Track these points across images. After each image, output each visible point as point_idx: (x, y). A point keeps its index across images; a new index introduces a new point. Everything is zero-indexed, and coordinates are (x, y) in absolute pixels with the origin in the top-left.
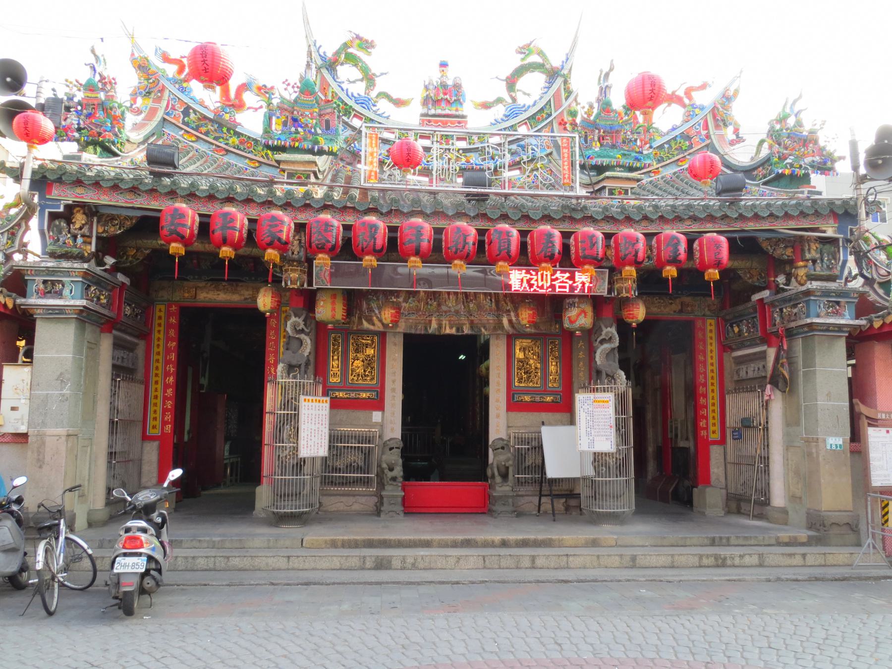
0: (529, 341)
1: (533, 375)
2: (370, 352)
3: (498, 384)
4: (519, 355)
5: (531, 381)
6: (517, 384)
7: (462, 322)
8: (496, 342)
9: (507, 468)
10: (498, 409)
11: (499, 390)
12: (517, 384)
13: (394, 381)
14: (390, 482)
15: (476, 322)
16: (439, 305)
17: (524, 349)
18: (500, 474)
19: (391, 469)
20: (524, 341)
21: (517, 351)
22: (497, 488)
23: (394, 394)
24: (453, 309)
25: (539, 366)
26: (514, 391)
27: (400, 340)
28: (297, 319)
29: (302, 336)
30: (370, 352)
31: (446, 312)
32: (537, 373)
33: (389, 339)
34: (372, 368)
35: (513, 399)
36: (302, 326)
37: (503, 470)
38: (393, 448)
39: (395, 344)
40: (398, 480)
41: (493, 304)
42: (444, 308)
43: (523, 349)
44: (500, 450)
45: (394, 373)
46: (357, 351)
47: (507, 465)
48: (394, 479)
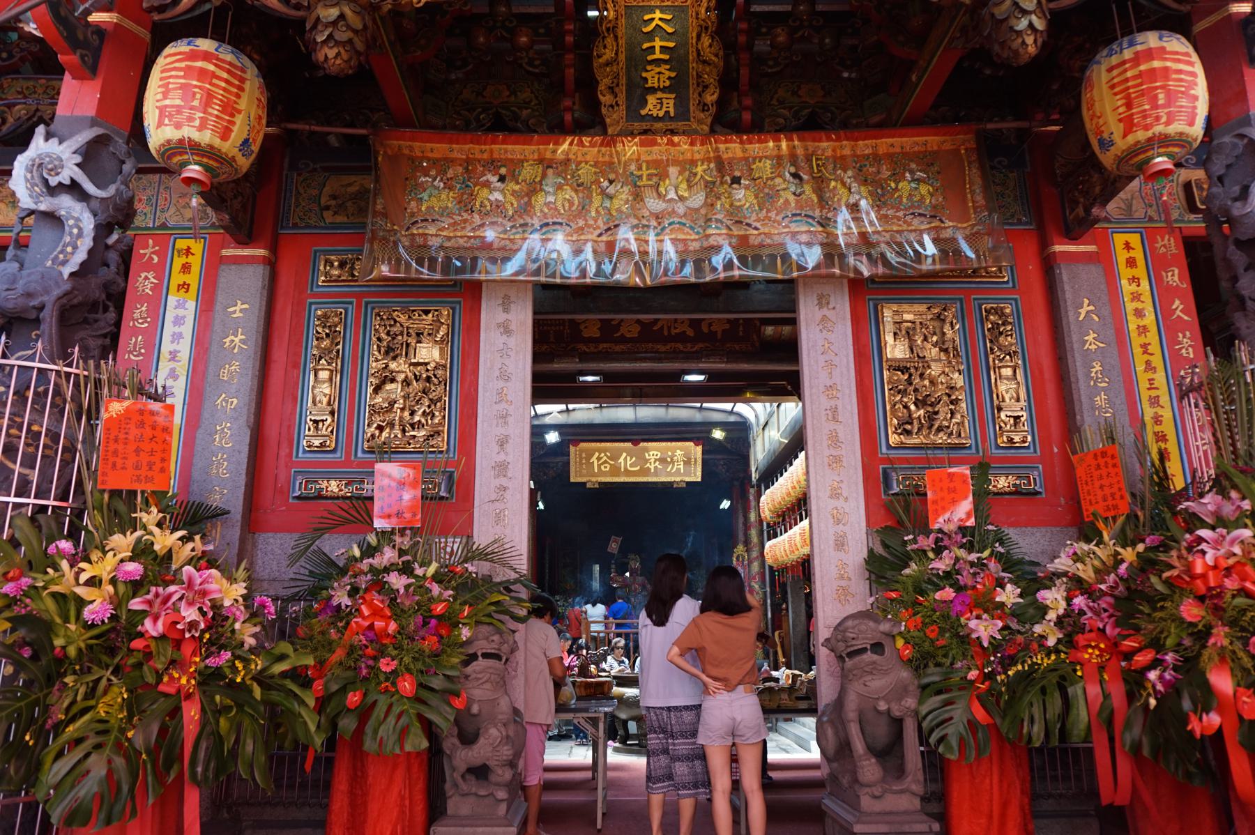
0: (922, 308)
1: (943, 410)
2: (428, 353)
3: (834, 440)
4: (896, 350)
5: (940, 429)
6: (894, 439)
7: (712, 241)
8: (819, 314)
9: (898, 723)
10: (838, 522)
11: (837, 460)
12: (894, 439)
13: (502, 443)
14: (464, 787)
15: (754, 241)
16: (638, 196)
17: (909, 335)
18: (872, 750)
19: (468, 738)
20: (905, 307)
21: (889, 339)
22: (866, 802)
23: (504, 482)
24: (681, 209)
25: (958, 380)
26: (889, 460)
27: (522, 318)
28: (53, 147)
29: (66, 204)
30: (428, 353)
31: (658, 217)
32: (955, 402)
33: (490, 314)
34: (433, 402)
35: (888, 485)
36: (70, 171)
37: (882, 732)
38: (473, 657)
39: (506, 329)
40: (493, 778)
41: (808, 189)
42: (653, 204)
43: (906, 333)
44: (869, 657)
45: (504, 417)
46: (390, 352)
47: (896, 713)
48: (480, 772)
